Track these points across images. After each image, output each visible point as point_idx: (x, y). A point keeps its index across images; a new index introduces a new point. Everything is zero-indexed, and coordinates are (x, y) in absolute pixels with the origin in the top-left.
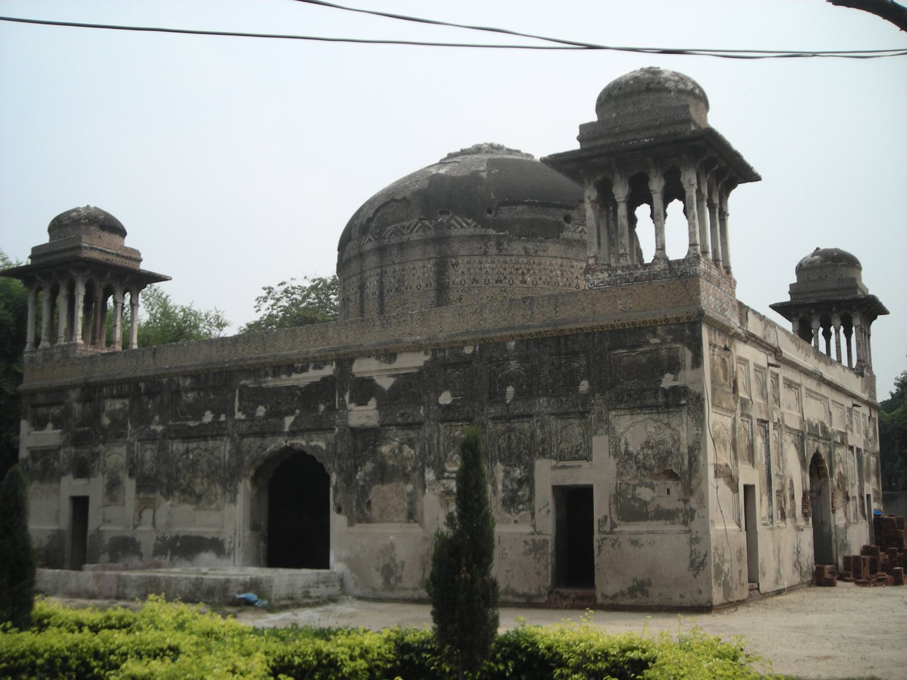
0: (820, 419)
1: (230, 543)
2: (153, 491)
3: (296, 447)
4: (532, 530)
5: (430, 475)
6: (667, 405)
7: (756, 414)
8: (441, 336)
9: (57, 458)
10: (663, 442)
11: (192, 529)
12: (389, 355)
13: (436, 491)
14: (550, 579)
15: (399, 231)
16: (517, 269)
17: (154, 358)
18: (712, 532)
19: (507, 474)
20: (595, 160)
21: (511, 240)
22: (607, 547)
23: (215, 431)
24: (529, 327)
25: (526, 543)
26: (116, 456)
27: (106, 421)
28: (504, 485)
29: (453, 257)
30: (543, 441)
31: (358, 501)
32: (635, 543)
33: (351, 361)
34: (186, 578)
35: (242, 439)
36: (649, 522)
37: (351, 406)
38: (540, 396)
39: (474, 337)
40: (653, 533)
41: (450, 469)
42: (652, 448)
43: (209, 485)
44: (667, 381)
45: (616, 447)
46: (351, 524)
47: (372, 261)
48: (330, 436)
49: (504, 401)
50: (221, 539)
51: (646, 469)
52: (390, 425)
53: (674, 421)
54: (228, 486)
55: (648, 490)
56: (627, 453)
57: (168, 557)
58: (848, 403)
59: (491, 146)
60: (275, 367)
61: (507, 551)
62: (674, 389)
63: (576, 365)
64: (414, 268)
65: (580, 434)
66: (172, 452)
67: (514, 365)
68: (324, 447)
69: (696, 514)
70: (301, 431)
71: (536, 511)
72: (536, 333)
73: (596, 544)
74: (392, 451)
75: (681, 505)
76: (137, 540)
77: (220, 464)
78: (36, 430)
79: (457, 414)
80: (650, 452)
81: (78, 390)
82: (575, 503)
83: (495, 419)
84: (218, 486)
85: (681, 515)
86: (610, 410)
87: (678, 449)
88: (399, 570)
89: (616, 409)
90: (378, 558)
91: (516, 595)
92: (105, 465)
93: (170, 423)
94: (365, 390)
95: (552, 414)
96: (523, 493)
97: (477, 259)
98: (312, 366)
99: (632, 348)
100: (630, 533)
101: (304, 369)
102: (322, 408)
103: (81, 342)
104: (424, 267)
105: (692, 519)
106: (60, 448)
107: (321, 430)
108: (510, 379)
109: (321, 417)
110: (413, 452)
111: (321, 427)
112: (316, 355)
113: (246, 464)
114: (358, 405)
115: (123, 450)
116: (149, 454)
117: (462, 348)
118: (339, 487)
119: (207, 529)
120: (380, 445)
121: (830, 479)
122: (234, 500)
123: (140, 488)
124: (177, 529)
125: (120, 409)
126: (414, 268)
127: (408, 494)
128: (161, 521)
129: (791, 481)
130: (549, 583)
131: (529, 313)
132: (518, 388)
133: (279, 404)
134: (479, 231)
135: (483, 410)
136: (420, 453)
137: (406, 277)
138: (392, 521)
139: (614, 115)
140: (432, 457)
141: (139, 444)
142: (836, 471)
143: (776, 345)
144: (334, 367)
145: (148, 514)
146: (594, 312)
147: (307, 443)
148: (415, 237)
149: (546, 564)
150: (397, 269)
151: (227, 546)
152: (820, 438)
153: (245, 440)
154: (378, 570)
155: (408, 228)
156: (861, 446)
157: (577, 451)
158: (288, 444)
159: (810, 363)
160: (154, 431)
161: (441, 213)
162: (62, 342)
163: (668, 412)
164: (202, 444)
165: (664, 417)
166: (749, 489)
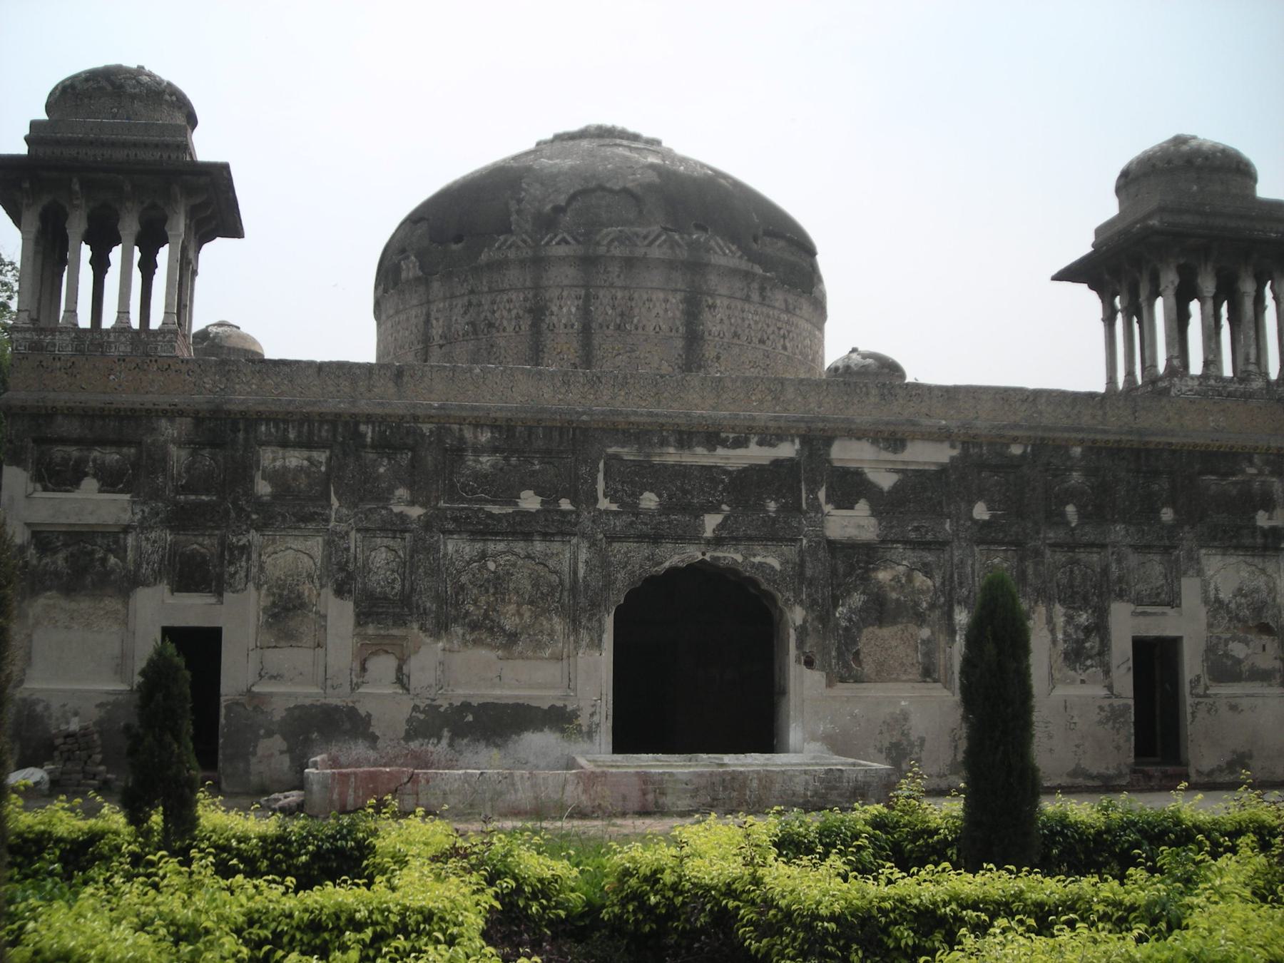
1: (592, 715)
2: (401, 621)
3: (722, 563)
4: (1105, 692)
6: (1265, 548)
8: (978, 423)
9: (121, 552)
10: (1257, 590)
11: (498, 692)
12: (895, 442)
14: (1132, 754)
15: (628, 238)
16: (779, 329)
19: (1070, 619)
23: (552, 526)
24: (1105, 432)
25: (1101, 708)
26: (293, 555)
28: (1065, 632)
29: (708, 294)
30: (1120, 579)
31: (838, 649)
32: (1233, 708)
33: (829, 441)
34: (805, 772)
35: (610, 543)
37: (828, 508)
38: (1115, 522)
39: (1031, 433)
40: (1252, 696)
42: (1245, 596)
44: (1262, 519)
45: (1206, 592)
46: (830, 684)
48: (790, 551)
49: (1068, 523)
50: (570, 708)
51: (1239, 621)
52: (898, 542)
54: (584, 622)
56: (1218, 600)
57: (444, 742)
59: (600, 128)
60: (680, 433)
62: (1274, 530)
63: (1156, 487)
66: (445, 555)
67: (1076, 477)
68: (777, 566)
71: (1114, 669)
72: (1115, 441)
73: (1189, 710)
74: (896, 579)
76: (363, 714)
77: (561, 582)
78: (45, 489)
80: (1243, 601)
81: (185, 424)
82: (1155, 659)
83: (1054, 546)
84: (556, 619)
86: (1202, 547)
87: (1274, 599)
88: (917, 749)
89: (1208, 547)
90: (881, 733)
91: (1092, 777)
92: (262, 568)
93: (442, 504)
94: (849, 487)
95: (1131, 546)
96: (1092, 644)
97: (739, 304)
98: (754, 439)
99: (1225, 475)
101: (740, 443)
102: (772, 506)
104: (666, 301)
106: (126, 529)
107: (773, 540)
109: (774, 521)
110: (929, 582)
111: (772, 536)
112: (770, 424)
113: (619, 585)
114: (838, 507)
115: (316, 545)
116: (381, 560)
117: (1008, 446)
118: (810, 629)
122: (597, 644)
123: (363, 617)
124: (460, 692)
125: (300, 469)
126: (650, 300)
127: (923, 642)
130: (1131, 760)
131: (1100, 413)
133: (685, 492)
134: (744, 265)
135: (1038, 533)
136: (943, 583)
137: (636, 311)
138: (896, 680)
139: (1195, 188)
140: (965, 591)
141: (359, 535)
144: (797, 446)
147: (745, 558)
148: (655, 253)
150: (619, 295)
151: (583, 720)
153: (615, 544)
154: (880, 751)
157: (1158, 595)
158: (707, 558)
160: (401, 516)
163: (1263, 556)
164: (519, 547)
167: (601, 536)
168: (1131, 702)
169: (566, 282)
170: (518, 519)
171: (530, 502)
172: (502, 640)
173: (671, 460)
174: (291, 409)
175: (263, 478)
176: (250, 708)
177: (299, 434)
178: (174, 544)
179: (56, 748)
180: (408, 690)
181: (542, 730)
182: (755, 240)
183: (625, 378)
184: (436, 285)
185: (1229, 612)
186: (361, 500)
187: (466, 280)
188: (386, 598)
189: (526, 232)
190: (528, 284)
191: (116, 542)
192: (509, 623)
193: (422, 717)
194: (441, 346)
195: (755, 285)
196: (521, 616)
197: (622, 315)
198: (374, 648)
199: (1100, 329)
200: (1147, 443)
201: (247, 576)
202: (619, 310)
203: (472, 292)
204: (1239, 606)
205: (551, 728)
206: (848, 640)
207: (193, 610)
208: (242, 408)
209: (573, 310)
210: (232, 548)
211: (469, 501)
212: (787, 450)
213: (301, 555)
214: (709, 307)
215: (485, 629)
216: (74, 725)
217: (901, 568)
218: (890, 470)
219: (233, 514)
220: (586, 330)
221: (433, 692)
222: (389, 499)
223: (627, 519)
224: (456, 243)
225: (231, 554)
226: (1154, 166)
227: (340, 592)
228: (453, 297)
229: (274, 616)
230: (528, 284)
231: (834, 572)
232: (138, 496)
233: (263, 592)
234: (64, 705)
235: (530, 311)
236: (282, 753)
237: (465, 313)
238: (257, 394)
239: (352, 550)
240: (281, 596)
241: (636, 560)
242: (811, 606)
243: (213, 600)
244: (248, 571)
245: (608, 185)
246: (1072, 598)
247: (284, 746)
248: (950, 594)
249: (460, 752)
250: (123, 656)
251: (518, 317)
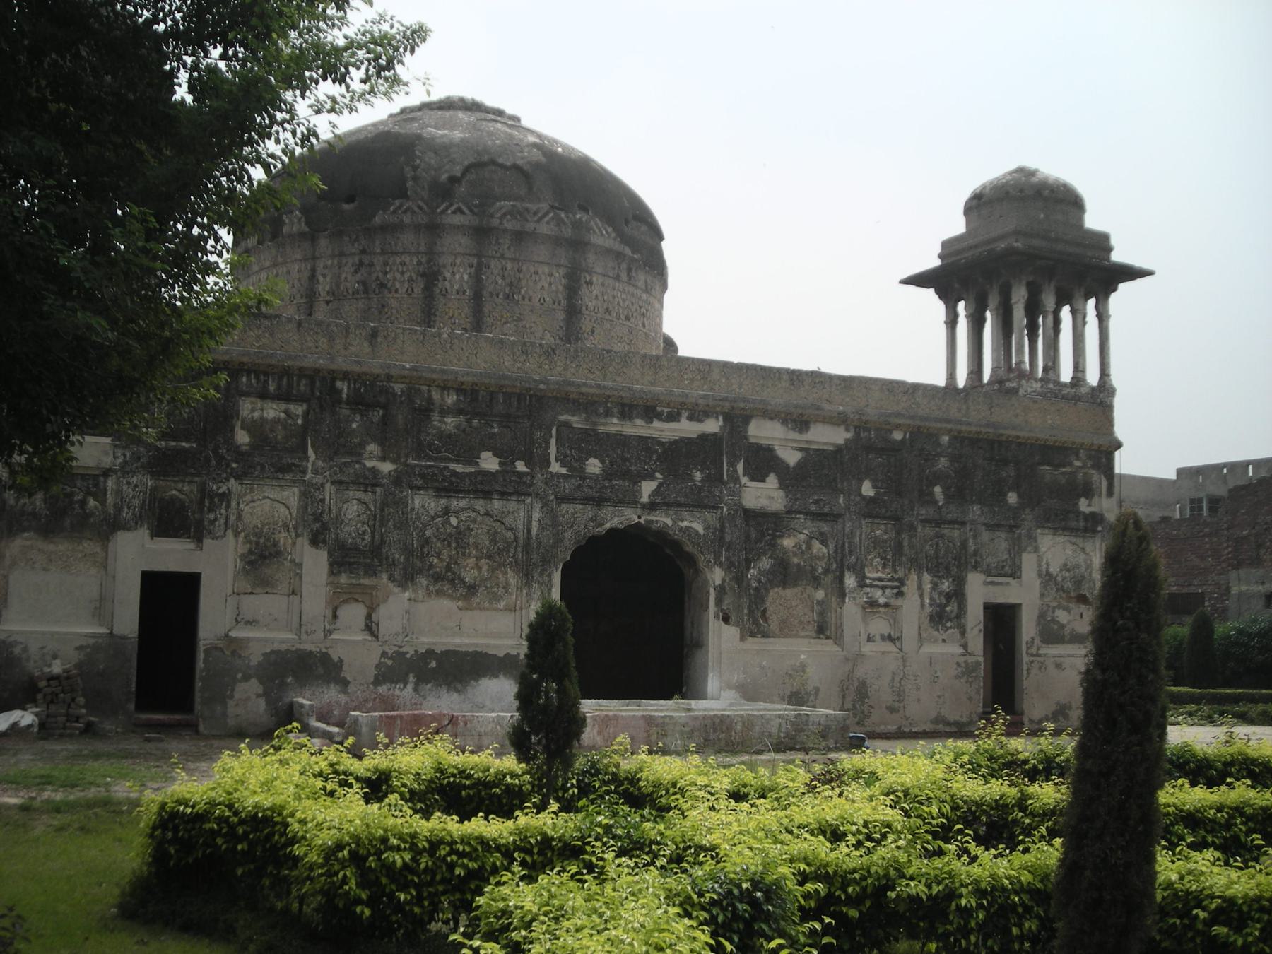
2: (372, 571)
4: (961, 650)
5: (850, 581)
6: (1086, 530)
9: (100, 495)
10: (1077, 566)
11: (457, 640)
12: (802, 424)
13: (858, 600)
19: (935, 586)
22: (1033, 671)
23: (508, 486)
24: (969, 424)
26: (270, 504)
27: (242, 438)
28: (931, 599)
30: (976, 553)
31: (749, 607)
32: (1058, 666)
33: (747, 420)
34: (779, 716)
36: (1066, 646)
37: (744, 480)
39: (908, 422)
40: (1073, 656)
42: (1069, 570)
43: (492, 570)
44: (1084, 506)
45: (1040, 566)
48: (711, 517)
49: (936, 502)
52: (800, 513)
53: (1088, 546)
56: (1048, 574)
57: (410, 687)
60: (623, 405)
61: (939, 674)
62: (1093, 514)
66: (413, 509)
67: (943, 462)
68: (701, 531)
70: (668, 505)
71: (968, 630)
73: (1025, 667)
74: (797, 546)
76: (336, 659)
77: (516, 539)
82: (1001, 620)
83: (925, 522)
84: (510, 574)
88: (812, 698)
91: (949, 724)
92: (239, 517)
93: (411, 461)
94: (762, 462)
96: (952, 608)
97: (611, 281)
98: (685, 414)
101: (673, 417)
102: (698, 476)
106: (107, 473)
107: (698, 506)
108: (936, 478)
109: (700, 489)
110: (824, 550)
111: (698, 503)
112: (700, 401)
113: (566, 543)
114: (753, 479)
115: (292, 496)
117: (891, 431)
119: (492, 642)
120: (781, 537)
124: (425, 639)
125: (277, 421)
133: (625, 460)
134: (617, 246)
135: (912, 509)
136: (836, 552)
137: (524, 282)
138: (797, 636)
144: (721, 423)
147: (674, 522)
148: (544, 229)
149: (977, 691)
150: (509, 266)
155: (535, 213)
157: (1003, 567)
158: (642, 521)
160: (374, 471)
164: (479, 504)
165: (1079, 541)
167: (552, 497)
168: (981, 659)
169: (460, 250)
170: (479, 478)
171: (489, 462)
172: (462, 591)
174: (273, 362)
175: (242, 428)
176: (228, 653)
177: (279, 387)
178: (154, 489)
179: (40, 690)
180: (377, 637)
181: (497, 677)
183: (576, 351)
184: (323, 243)
185: (1056, 584)
186: (336, 453)
187: (357, 240)
188: (356, 549)
189: (422, 199)
190: (422, 249)
191: (96, 485)
192: (469, 576)
193: (390, 662)
194: (328, 302)
195: (624, 266)
196: (480, 569)
197: (511, 285)
198: (345, 597)
199: (942, 331)
200: (1001, 435)
201: (226, 523)
202: (508, 281)
203: (363, 252)
204: (1064, 579)
205: (505, 675)
206: (758, 598)
207: (172, 555)
208: (226, 358)
209: (466, 277)
210: (212, 496)
211: (435, 459)
212: (712, 426)
213: (276, 504)
214: (587, 283)
215: (448, 581)
216: (57, 668)
217: (802, 536)
219: (213, 462)
220: (477, 297)
221: (400, 638)
222: (361, 454)
223: (575, 482)
224: (348, 202)
225: (212, 501)
226: (1007, 193)
227: (315, 542)
228: (342, 254)
229: (251, 563)
230: (422, 249)
231: (748, 537)
232: (119, 440)
233: (241, 539)
234: (42, 648)
235: (423, 275)
236: (258, 696)
237: (356, 272)
238: (239, 345)
239: (327, 502)
240: (257, 543)
241: (582, 521)
242: (729, 568)
243: (192, 546)
244: (227, 519)
245: (500, 161)
246: (938, 568)
247: (261, 691)
248: (842, 560)
249: (424, 697)
250: (102, 598)
251: (411, 280)
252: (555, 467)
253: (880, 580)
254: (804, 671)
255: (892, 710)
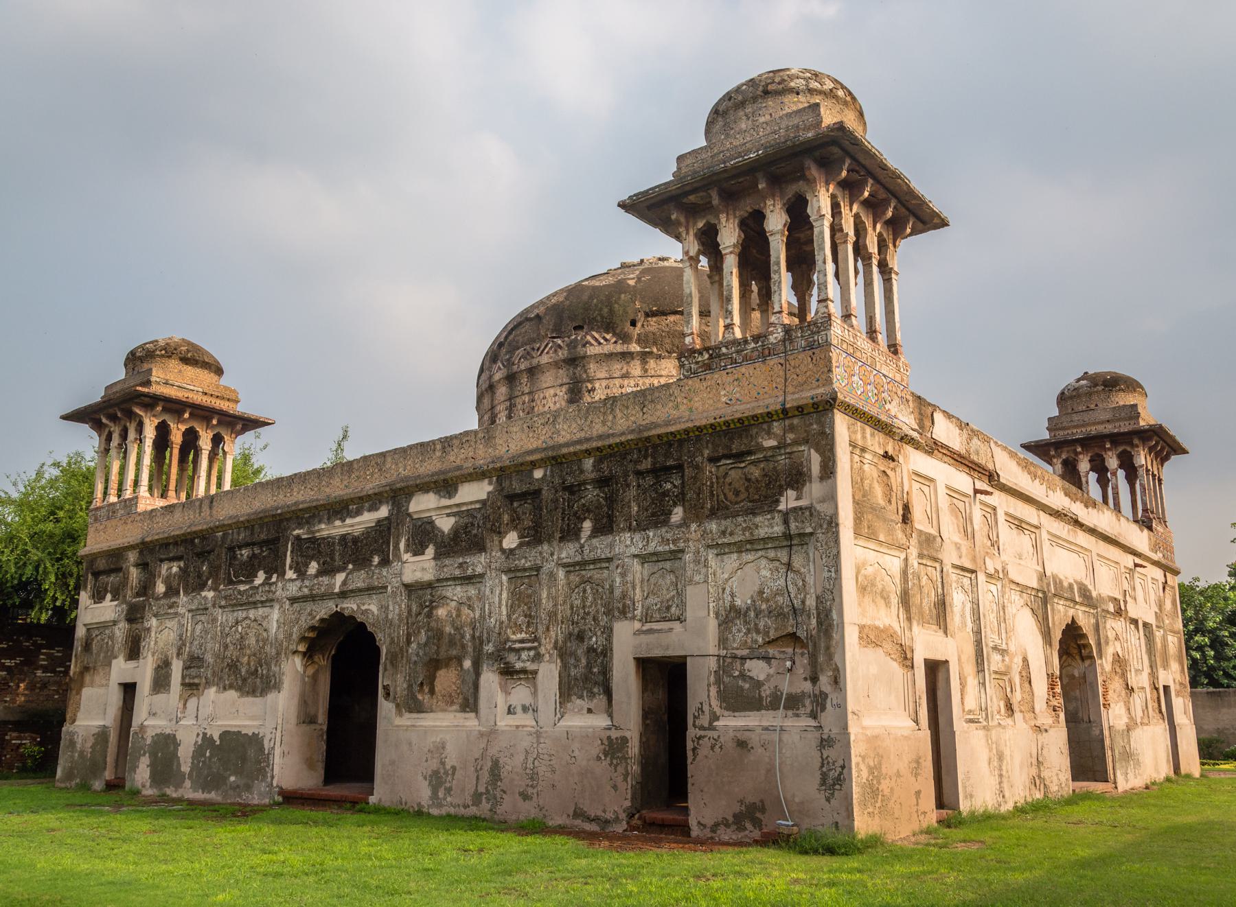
0: (1078, 579)
3: (346, 613)
7: (950, 557)
17: (211, 508)
18: (853, 730)
20: (692, 198)
21: (659, 357)
22: (704, 751)
24: (609, 436)
29: (589, 381)
36: (763, 712)
37: (406, 557)
41: (513, 637)
47: (502, 391)
55: (761, 664)
58: (1129, 560)
61: (576, 753)
63: (669, 486)
64: (544, 398)
65: (672, 583)
69: (829, 701)
73: (690, 745)
74: (449, 614)
75: (807, 686)
79: (523, 561)
85: (807, 702)
94: (423, 535)
97: (617, 382)
100: (737, 729)
101: (358, 512)
103: (147, 495)
105: (823, 709)
114: (415, 555)
121: (1098, 662)
126: (544, 398)
128: (204, 713)
129: (1025, 660)
131: (610, 418)
132: (596, 521)
134: (619, 348)
135: (552, 554)
142: (1110, 651)
143: (990, 466)
145: (192, 703)
146: (691, 410)
148: (545, 359)
152: (1076, 603)
154: (425, 778)
156: (1151, 619)
157: (668, 608)
159: (1058, 499)
161: (575, 328)
162: (128, 494)
164: (252, 614)
166: (935, 669)
173: (325, 533)
182: (633, 323)
212: (384, 512)
218: (448, 515)
252: (290, 574)
253: (522, 641)
254: (443, 748)
255: (525, 797)
